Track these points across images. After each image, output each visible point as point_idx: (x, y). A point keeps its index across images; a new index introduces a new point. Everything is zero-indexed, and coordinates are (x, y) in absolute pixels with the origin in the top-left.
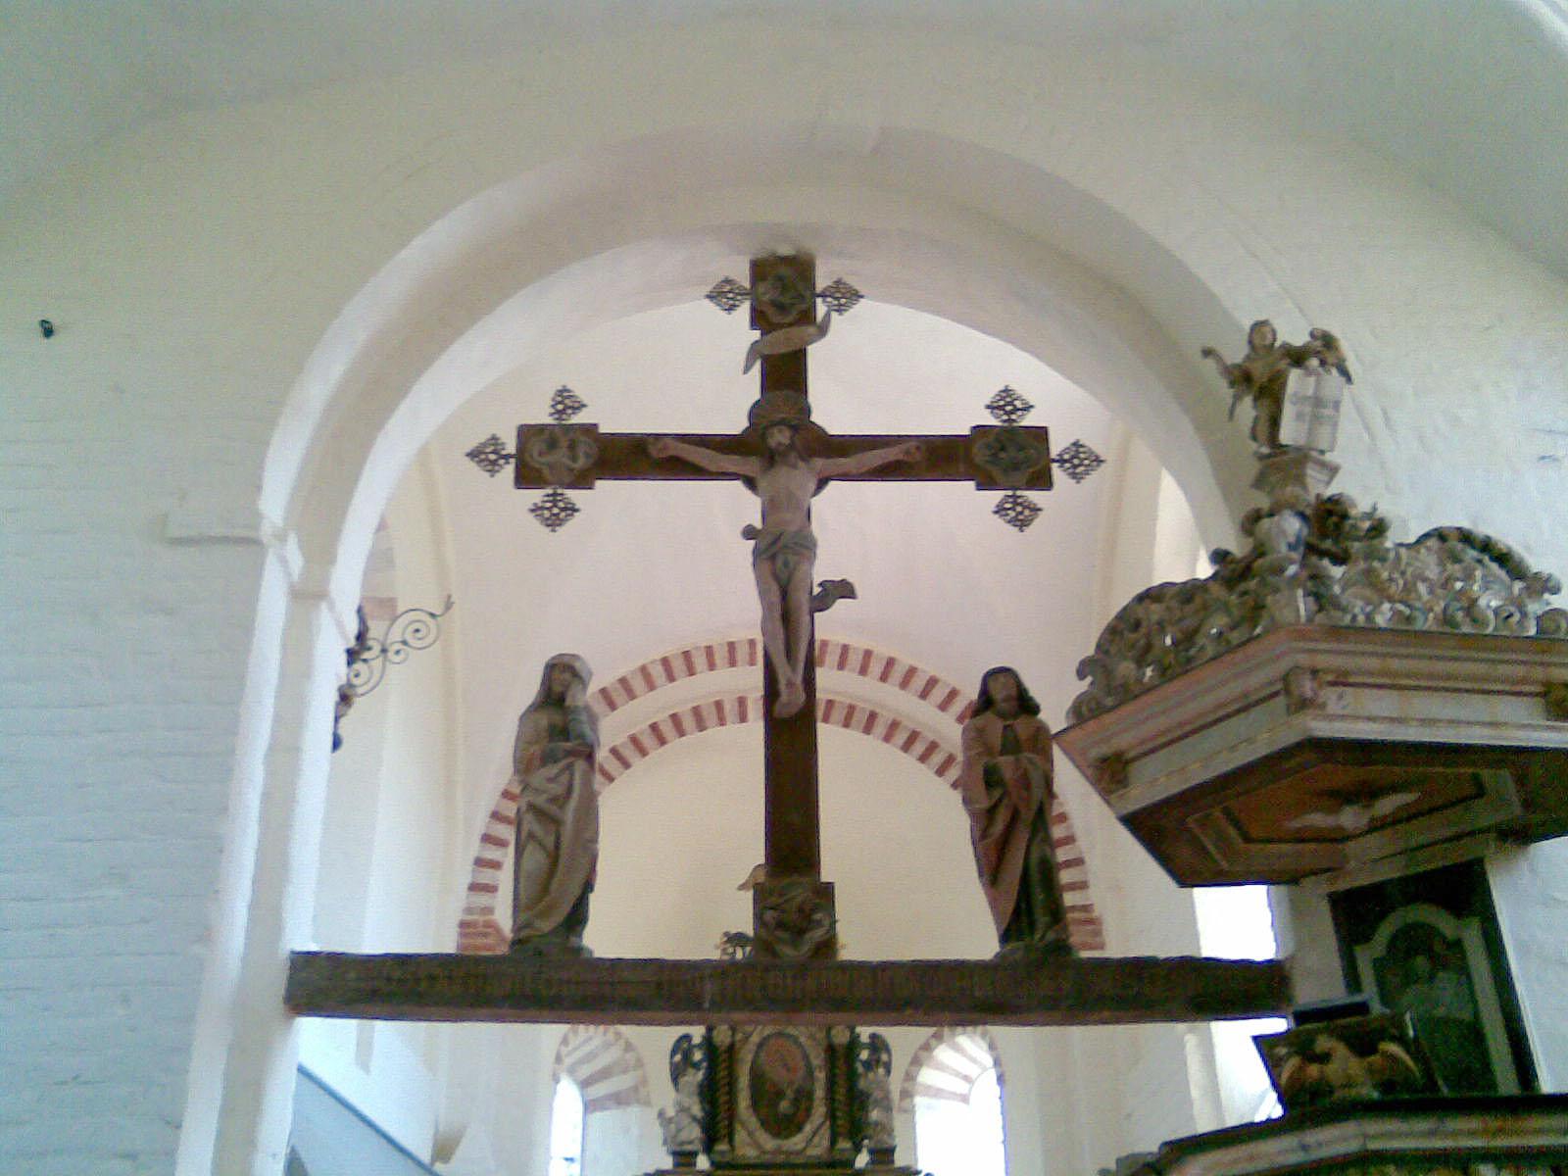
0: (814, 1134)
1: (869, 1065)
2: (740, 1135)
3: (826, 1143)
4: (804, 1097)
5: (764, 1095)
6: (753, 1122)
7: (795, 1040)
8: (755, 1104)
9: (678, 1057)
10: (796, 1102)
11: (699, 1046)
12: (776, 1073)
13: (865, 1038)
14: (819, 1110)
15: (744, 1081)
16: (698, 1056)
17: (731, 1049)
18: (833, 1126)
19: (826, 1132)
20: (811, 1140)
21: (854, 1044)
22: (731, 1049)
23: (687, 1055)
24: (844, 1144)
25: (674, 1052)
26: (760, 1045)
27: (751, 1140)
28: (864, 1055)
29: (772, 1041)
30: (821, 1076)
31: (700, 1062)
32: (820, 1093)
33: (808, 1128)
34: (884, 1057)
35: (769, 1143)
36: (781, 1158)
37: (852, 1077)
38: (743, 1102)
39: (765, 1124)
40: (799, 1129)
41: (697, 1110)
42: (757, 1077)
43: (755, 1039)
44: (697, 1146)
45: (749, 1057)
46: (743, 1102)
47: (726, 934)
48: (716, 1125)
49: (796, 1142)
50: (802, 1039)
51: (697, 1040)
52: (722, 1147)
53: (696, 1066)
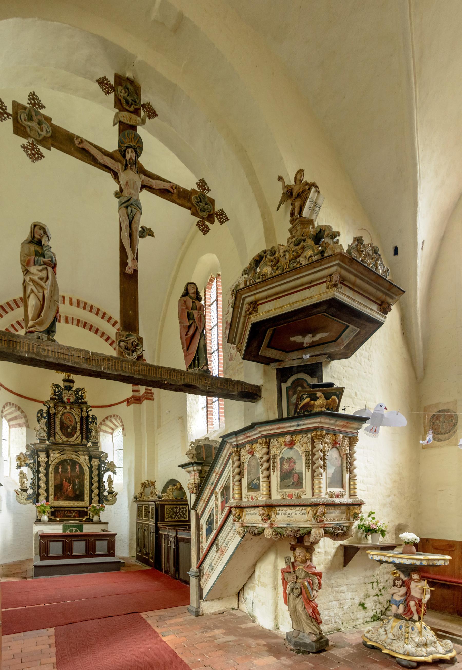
0: (77, 438)
1: (91, 423)
2: (57, 436)
3: (80, 440)
4: (74, 428)
5: (63, 427)
6: (60, 434)
7: (72, 414)
8: (61, 429)
9: (39, 415)
10: (72, 429)
11: (45, 413)
12: (67, 422)
13: (91, 416)
14: (78, 432)
15: (58, 423)
16: (45, 415)
17: (55, 414)
18: (82, 436)
19: (80, 437)
20: (76, 439)
21: (88, 417)
22: (55, 414)
23: (42, 415)
24: (84, 440)
25: (38, 413)
26: (62, 415)
27: (60, 438)
28: (90, 420)
29: (66, 414)
30: (79, 423)
31: (46, 417)
32: (78, 428)
33: (75, 436)
34: (95, 421)
35: (65, 439)
36: (68, 443)
37: (87, 425)
38: (58, 428)
39: (64, 434)
40: (73, 436)
41: (45, 429)
42: (62, 423)
43: (61, 412)
44: (46, 438)
45: (60, 417)
46: (58, 428)
47: (53, 384)
48: (51, 433)
49: (72, 439)
50: (74, 414)
51: (45, 411)
52: (52, 439)
53: (45, 418)
